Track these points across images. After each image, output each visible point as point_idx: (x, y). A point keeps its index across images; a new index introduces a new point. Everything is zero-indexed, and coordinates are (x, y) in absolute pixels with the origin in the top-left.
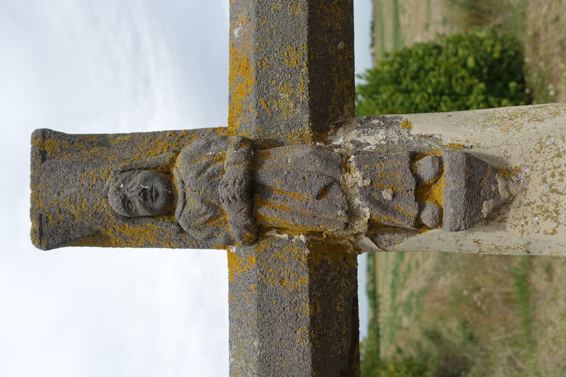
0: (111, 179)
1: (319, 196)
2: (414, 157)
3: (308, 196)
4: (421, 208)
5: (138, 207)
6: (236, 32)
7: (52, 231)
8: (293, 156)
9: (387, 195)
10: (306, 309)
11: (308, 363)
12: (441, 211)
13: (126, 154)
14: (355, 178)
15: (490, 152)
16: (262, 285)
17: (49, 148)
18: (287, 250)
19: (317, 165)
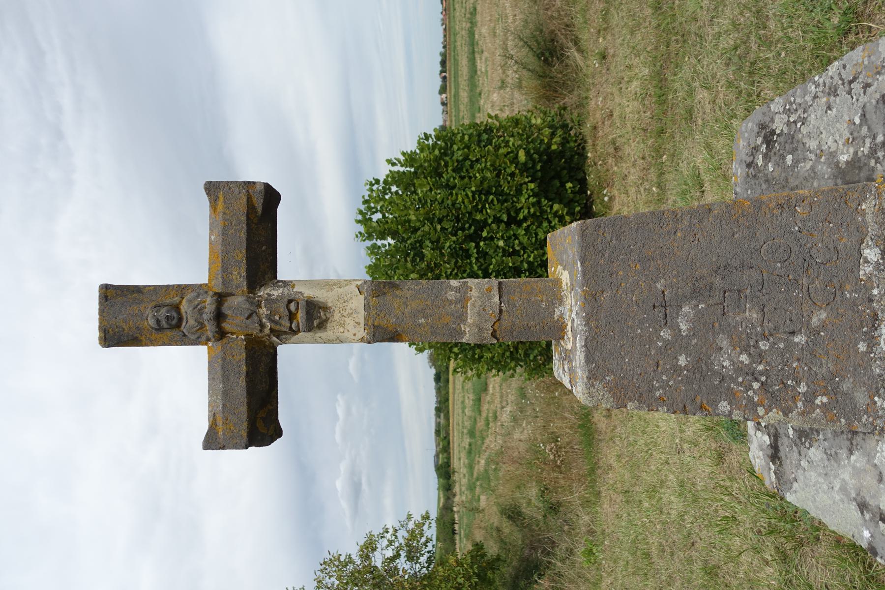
0: (148, 311)
1: (247, 318)
2: (290, 301)
3: (243, 318)
4: (291, 323)
5: (164, 324)
6: (213, 237)
7: (112, 337)
8: (237, 302)
9: (277, 318)
10: (244, 368)
11: (245, 392)
12: (298, 324)
13: (154, 298)
14: (264, 311)
15: (322, 300)
16: (224, 359)
17: (111, 296)
18: (235, 342)
19: (247, 306)
